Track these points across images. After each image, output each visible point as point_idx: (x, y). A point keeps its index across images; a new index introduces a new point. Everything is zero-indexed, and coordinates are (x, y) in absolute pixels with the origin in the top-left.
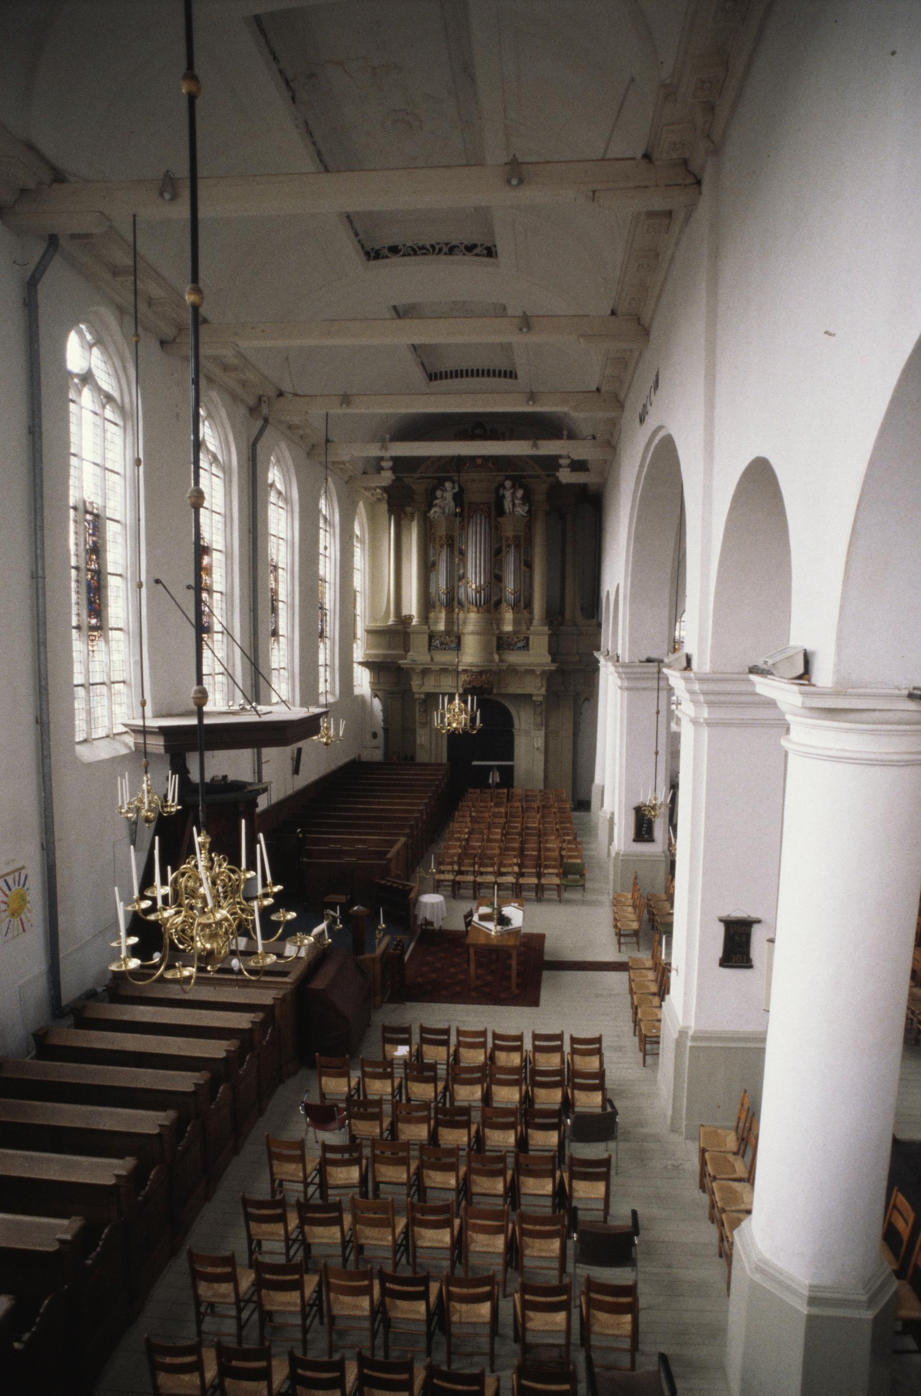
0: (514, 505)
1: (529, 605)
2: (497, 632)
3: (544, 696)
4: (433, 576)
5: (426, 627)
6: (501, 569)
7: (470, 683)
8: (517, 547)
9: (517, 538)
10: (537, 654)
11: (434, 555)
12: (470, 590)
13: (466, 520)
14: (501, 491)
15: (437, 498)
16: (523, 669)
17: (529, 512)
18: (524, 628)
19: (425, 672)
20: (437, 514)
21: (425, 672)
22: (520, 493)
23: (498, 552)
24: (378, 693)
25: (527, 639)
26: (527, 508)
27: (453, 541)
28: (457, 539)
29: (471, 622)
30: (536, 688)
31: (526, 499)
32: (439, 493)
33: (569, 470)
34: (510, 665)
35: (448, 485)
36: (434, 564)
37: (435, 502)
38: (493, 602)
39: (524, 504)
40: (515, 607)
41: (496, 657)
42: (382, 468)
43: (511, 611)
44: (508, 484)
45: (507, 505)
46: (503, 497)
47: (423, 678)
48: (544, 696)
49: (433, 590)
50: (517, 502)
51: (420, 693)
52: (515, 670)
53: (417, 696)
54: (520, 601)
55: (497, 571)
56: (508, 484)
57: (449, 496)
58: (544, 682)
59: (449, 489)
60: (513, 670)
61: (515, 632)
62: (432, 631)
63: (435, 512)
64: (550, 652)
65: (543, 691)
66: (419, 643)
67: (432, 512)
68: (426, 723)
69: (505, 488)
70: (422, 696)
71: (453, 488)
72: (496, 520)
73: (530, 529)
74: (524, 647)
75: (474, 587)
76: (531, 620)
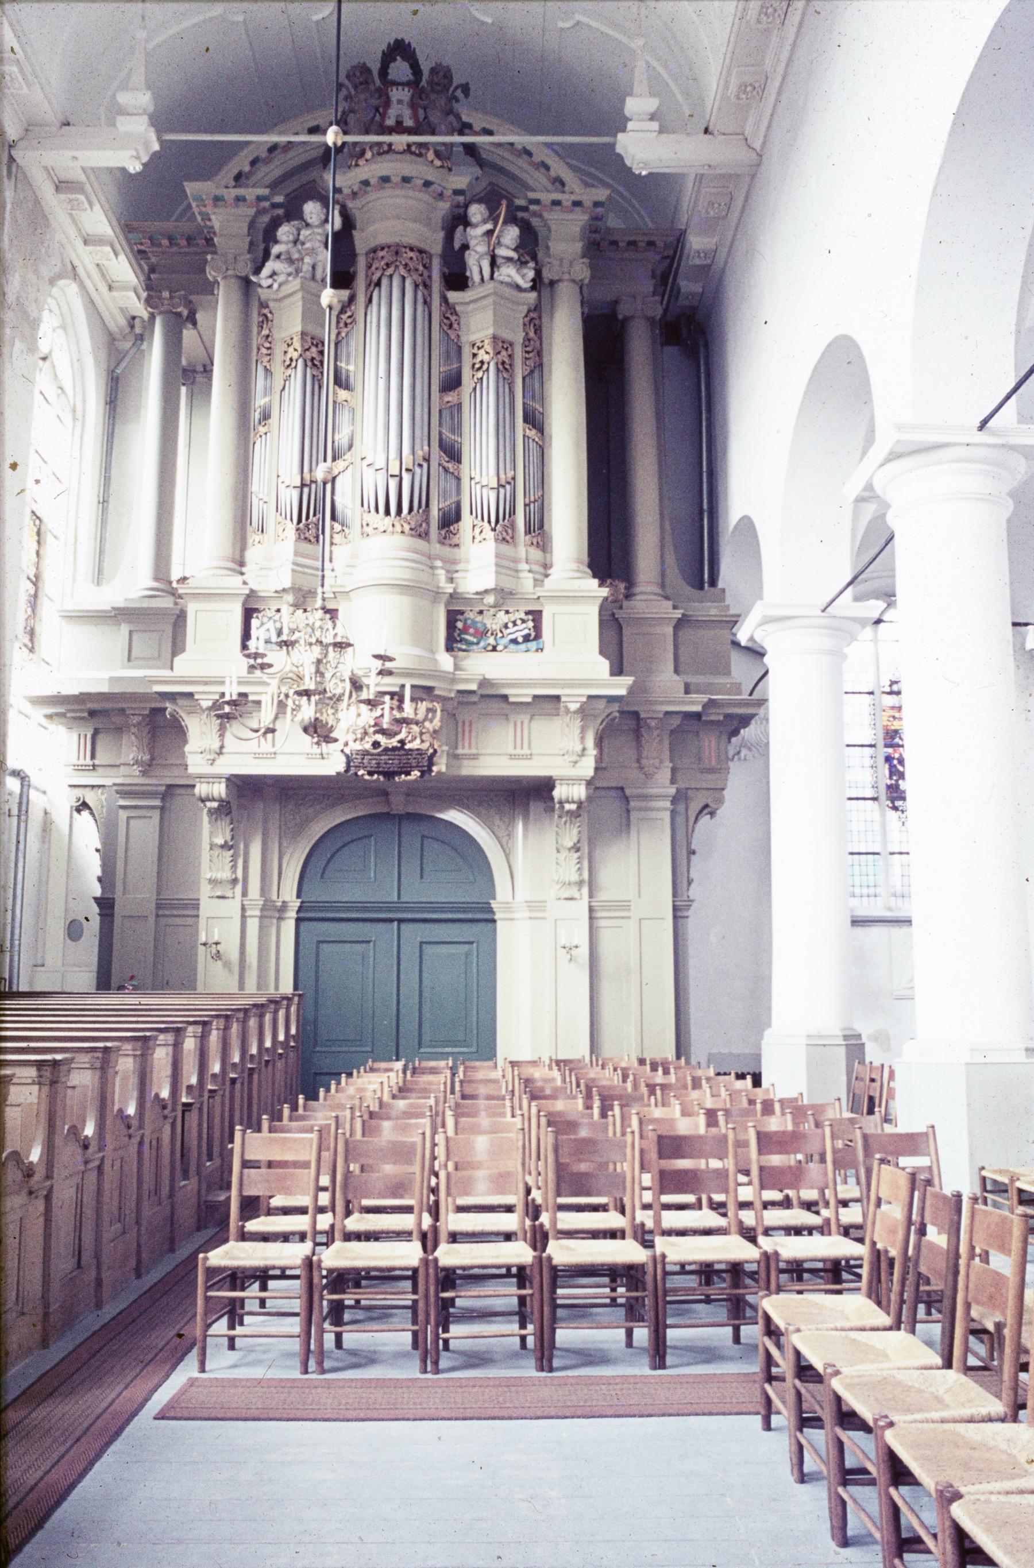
0: (493, 264)
1: (538, 528)
2: (449, 589)
3: (589, 783)
4: (259, 452)
5: (236, 581)
6: (457, 428)
8: (505, 368)
9: (501, 344)
10: (571, 655)
11: (268, 391)
12: (369, 475)
13: (361, 299)
14: (461, 228)
16: (524, 695)
17: (537, 284)
18: (527, 581)
19: (231, 711)
20: (281, 278)
21: (231, 711)
22: (511, 234)
23: (452, 383)
24: (90, 798)
25: (536, 616)
26: (531, 274)
27: (322, 353)
28: (328, 350)
29: (371, 556)
30: (562, 755)
31: (530, 246)
32: (285, 232)
33: (655, 125)
34: (484, 683)
35: (311, 209)
36: (266, 416)
38: (434, 512)
39: (522, 263)
40: (502, 524)
41: (446, 661)
42: (123, 112)
43: (490, 535)
44: (476, 212)
45: (476, 262)
47: (222, 736)
48: (589, 783)
49: (260, 486)
50: (502, 252)
52: (505, 697)
53: (202, 789)
54: (513, 512)
55: (447, 434)
56: (476, 212)
58: (590, 741)
60: (492, 700)
61: (504, 595)
62: (252, 595)
63: (273, 274)
64: (602, 652)
65: (587, 767)
66: (213, 629)
67: (266, 271)
68: (235, 881)
69: (467, 223)
70: (220, 789)
72: (445, 300)
73: (538, 330)
74: (527, 639)
75: (381, 463)
76: (546, 566)
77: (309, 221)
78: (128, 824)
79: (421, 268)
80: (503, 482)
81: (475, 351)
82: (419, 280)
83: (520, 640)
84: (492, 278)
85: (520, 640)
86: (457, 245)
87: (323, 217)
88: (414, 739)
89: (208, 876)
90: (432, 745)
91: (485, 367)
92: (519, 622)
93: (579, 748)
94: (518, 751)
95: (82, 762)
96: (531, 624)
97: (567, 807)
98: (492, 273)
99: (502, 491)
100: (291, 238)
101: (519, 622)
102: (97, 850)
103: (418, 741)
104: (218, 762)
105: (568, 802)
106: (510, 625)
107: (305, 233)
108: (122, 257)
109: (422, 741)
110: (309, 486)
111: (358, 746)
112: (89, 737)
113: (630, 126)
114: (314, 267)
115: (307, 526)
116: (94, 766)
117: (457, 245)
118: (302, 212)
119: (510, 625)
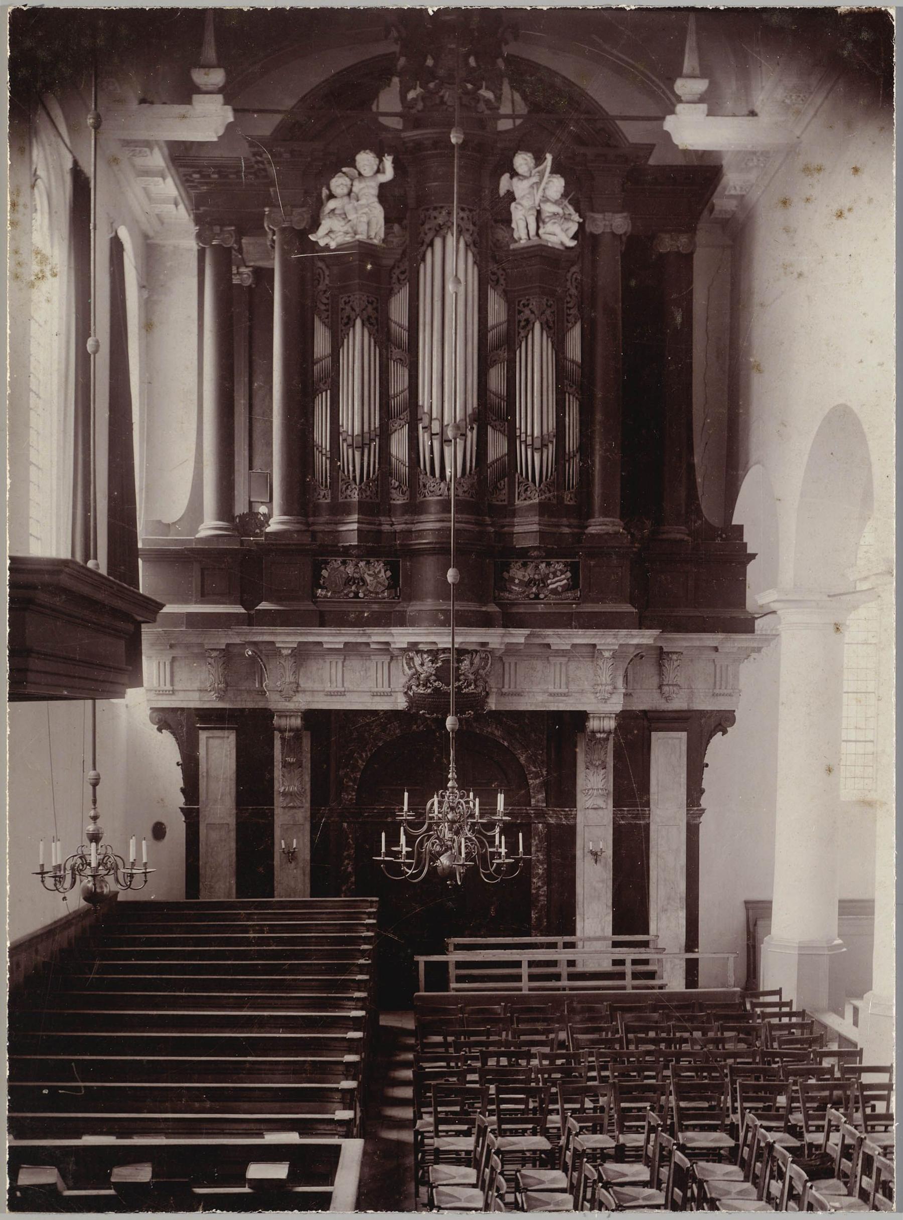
7: (427, 680)
14: (505, 179)
15: (331, 196)
35: (366, 160)
37: (331, 204)
46: (511, 196)
50: (549, 209)
51: (284, 714)
52: (548, 646)
57: (368, 190)
59: (367, 171)
63: (331, 231)
67: (322, 231)
69: (514, 174)
71: (378, 171)
75: (436, 428)
77: (362, 172)
78: (207, 741)
79: (471, 227)
80: (545, 443)
81: (521, 308)
82: (470, 240)
83: (560, 589)
84: (537, 234)
85: (560, 589)
86: (502, 191)
87: (375, 168)
88: (469, 685)
89: (282, 790)
90: (484, 689)
91: (530, 326)
92: (559, 573)
93: (609, 688)
94: (558, 690)
95: (163, 687)
96: (569, 574)
97: (598, 735)
98: (538, 228)
99: (545, 451)
100: (346, 191)
101: (559, 573)
102: (178, 764)
103: (473, 687)
104: (295, 699)
105: (600, 732)
106: (551, 576)
107: (357, 186)
108: (181, 207)
109: (476, 686)
110: (370, 445)
111: (421, 690)
112: (167, 663)
113: (680, 108)
114: (369, 224)
115: (367, 485)
116: (173, 691)
117: (502, 191)
118: (354, 161)
119: (551, 576)
